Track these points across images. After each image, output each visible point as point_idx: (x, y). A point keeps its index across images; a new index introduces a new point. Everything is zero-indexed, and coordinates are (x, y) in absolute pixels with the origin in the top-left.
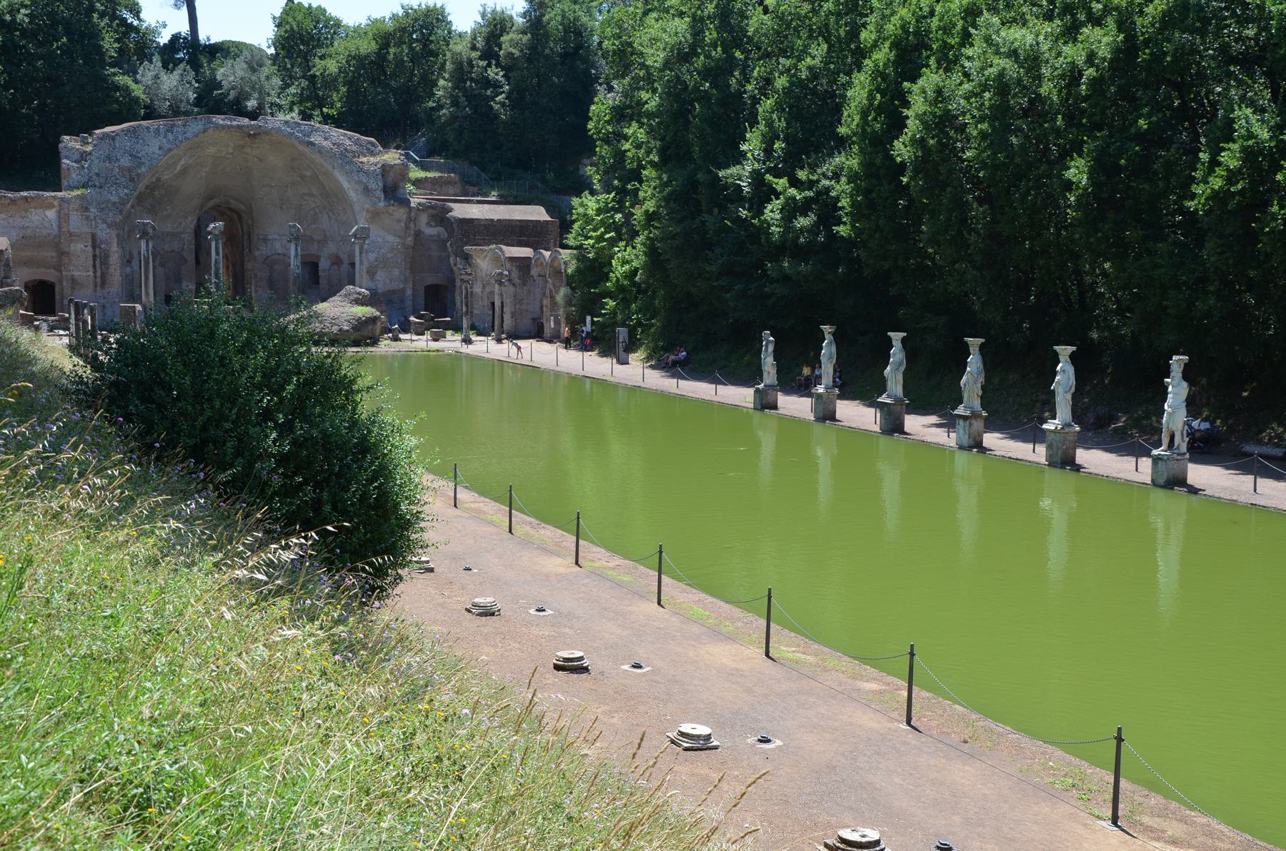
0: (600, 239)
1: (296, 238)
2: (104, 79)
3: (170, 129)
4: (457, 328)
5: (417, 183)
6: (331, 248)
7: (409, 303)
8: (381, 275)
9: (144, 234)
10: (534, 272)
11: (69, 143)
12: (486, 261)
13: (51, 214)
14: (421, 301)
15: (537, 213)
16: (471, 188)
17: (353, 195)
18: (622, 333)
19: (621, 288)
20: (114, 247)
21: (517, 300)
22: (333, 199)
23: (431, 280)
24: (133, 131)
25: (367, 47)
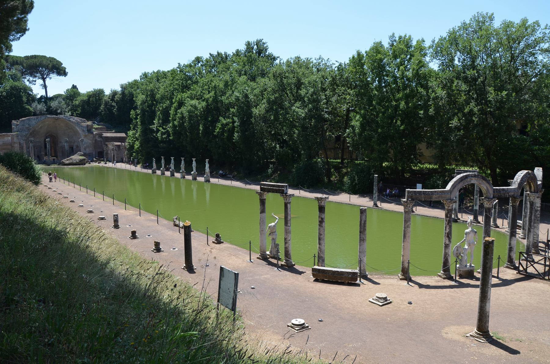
0: (132, 140)
1: (67, 142)
2: (23, 107)
3: (37, 118)
4: (103, 161)
5: (96, 129)
6: (76, 144)
7: (94, 156)
8: (87, 150)
9: (31, 142)
10: (121, 148)
11: (14, 122)
12: (111, 146)
13: (10, 138)
14: (97, 155)
15: (123, 135)
16: (108, 129)
17: (80, 132)
18: (136, 160)
19: (137, 151)
20: (25, 145)
21: (117, 154)
22: (76, 133)
23: (99, 150)
24: (28, 119)
25: (85, 98)
